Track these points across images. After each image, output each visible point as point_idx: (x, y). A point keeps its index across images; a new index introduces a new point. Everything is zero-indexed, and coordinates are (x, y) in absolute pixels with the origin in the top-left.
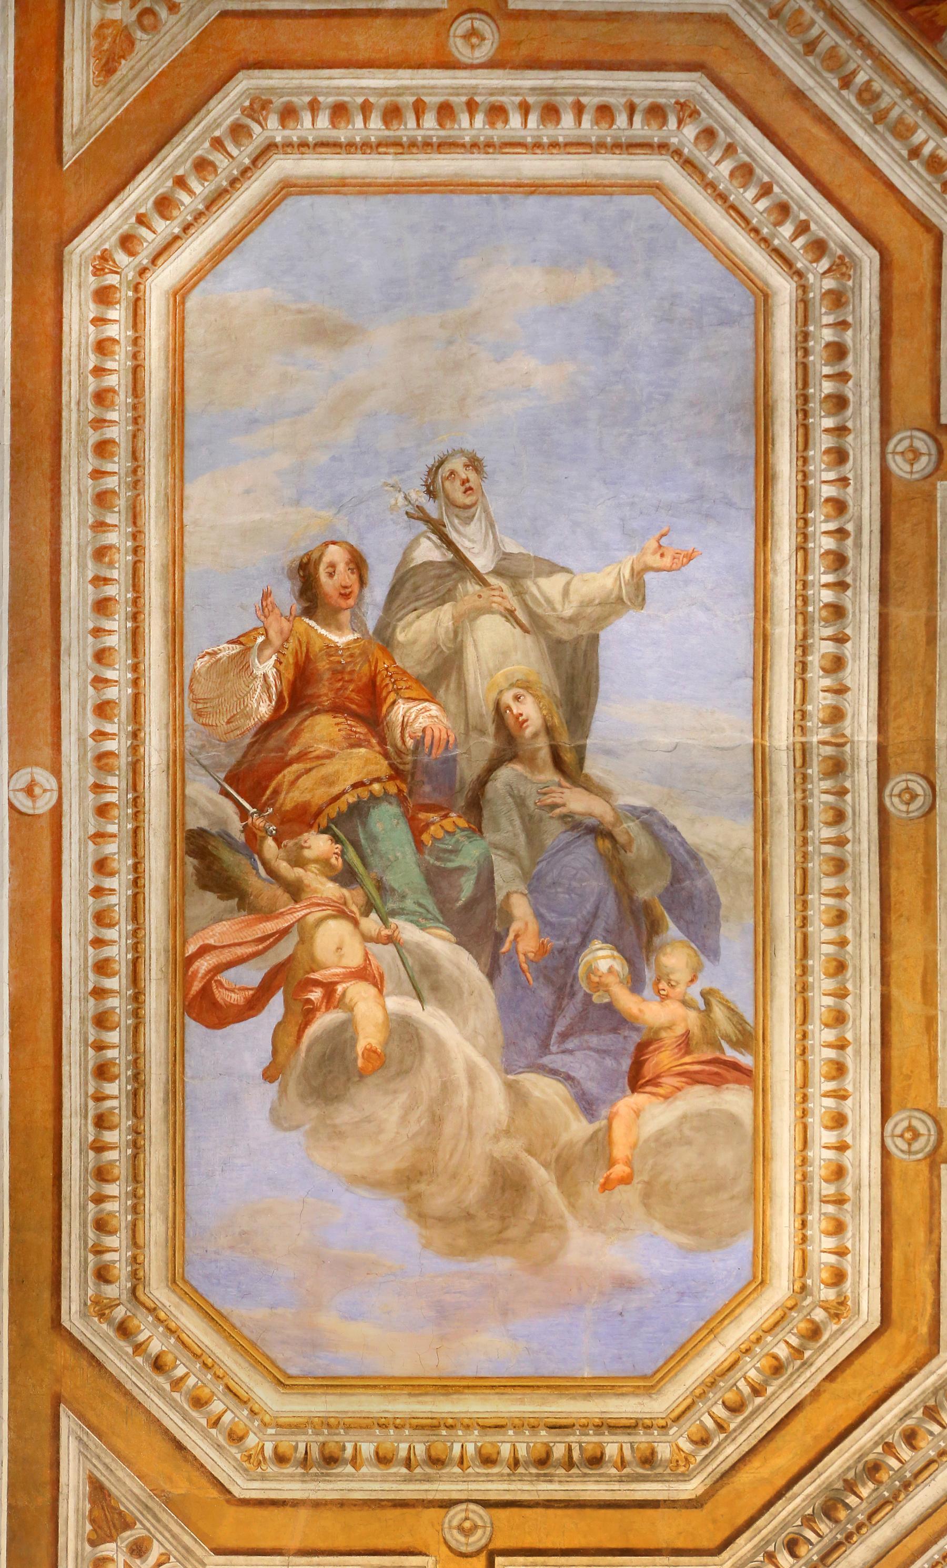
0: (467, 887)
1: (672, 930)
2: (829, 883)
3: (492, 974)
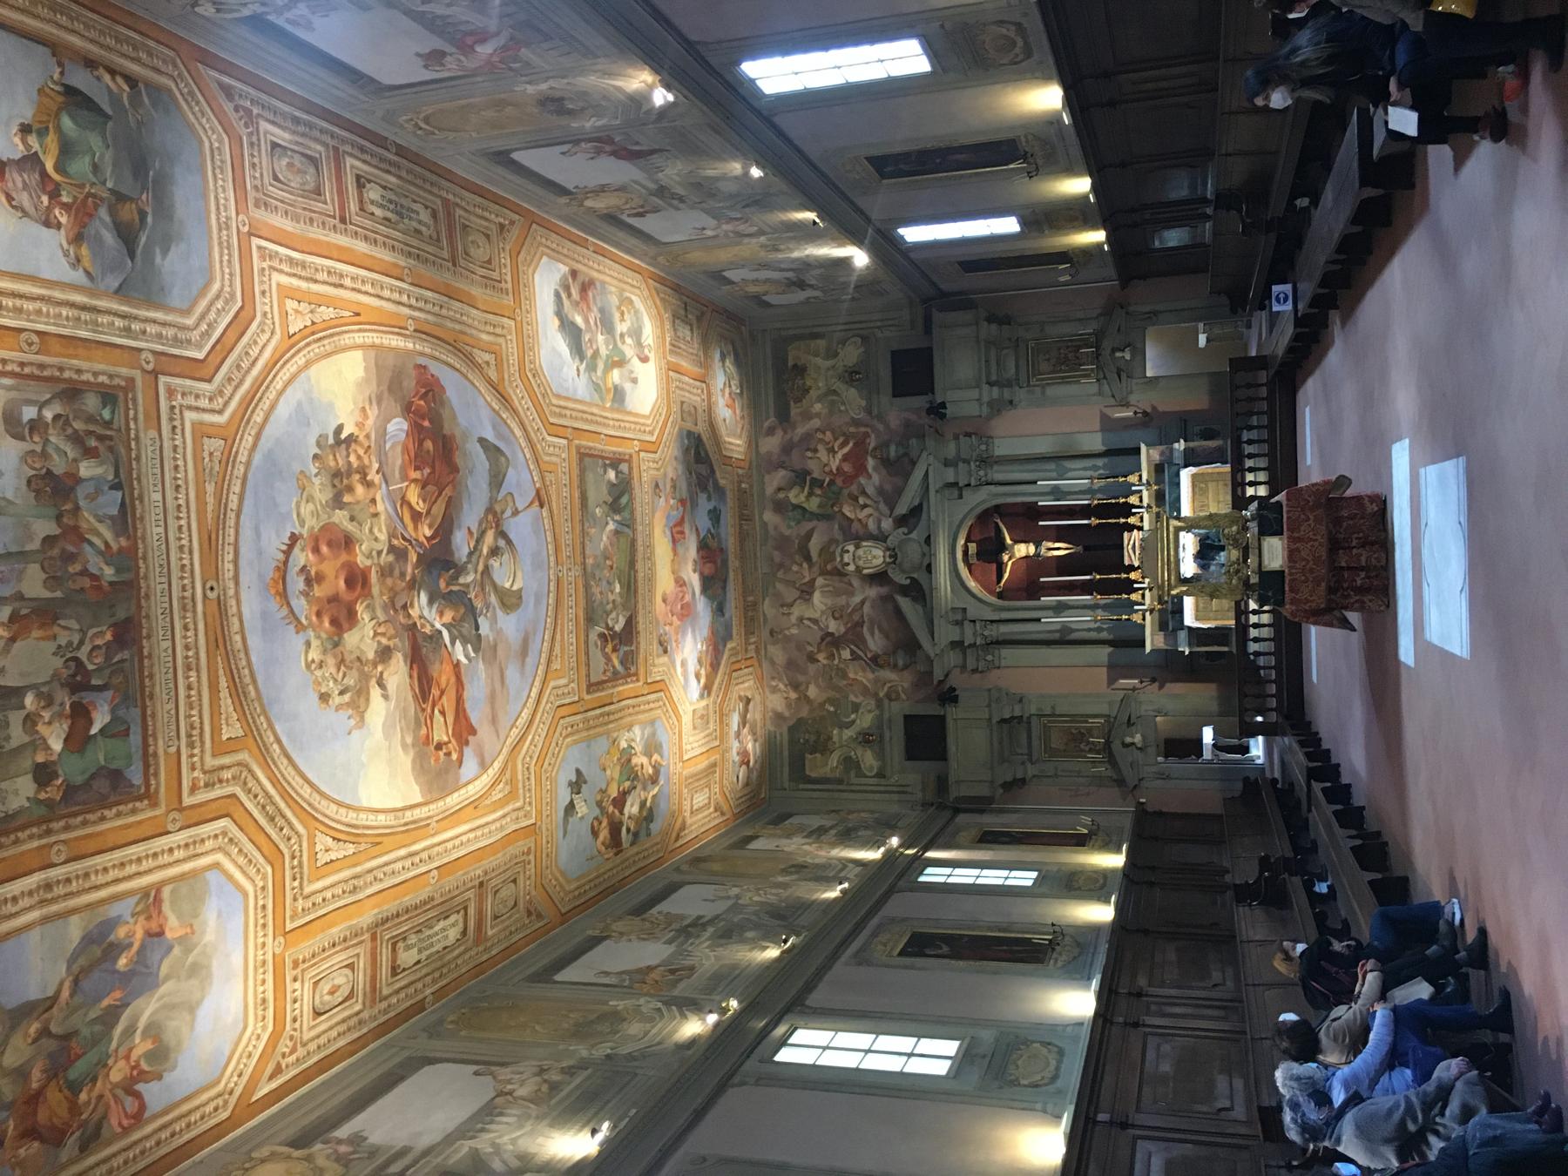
0: (97, 1028)
1: (112, 937)
2: (93, 877)
3: (128, 1005)
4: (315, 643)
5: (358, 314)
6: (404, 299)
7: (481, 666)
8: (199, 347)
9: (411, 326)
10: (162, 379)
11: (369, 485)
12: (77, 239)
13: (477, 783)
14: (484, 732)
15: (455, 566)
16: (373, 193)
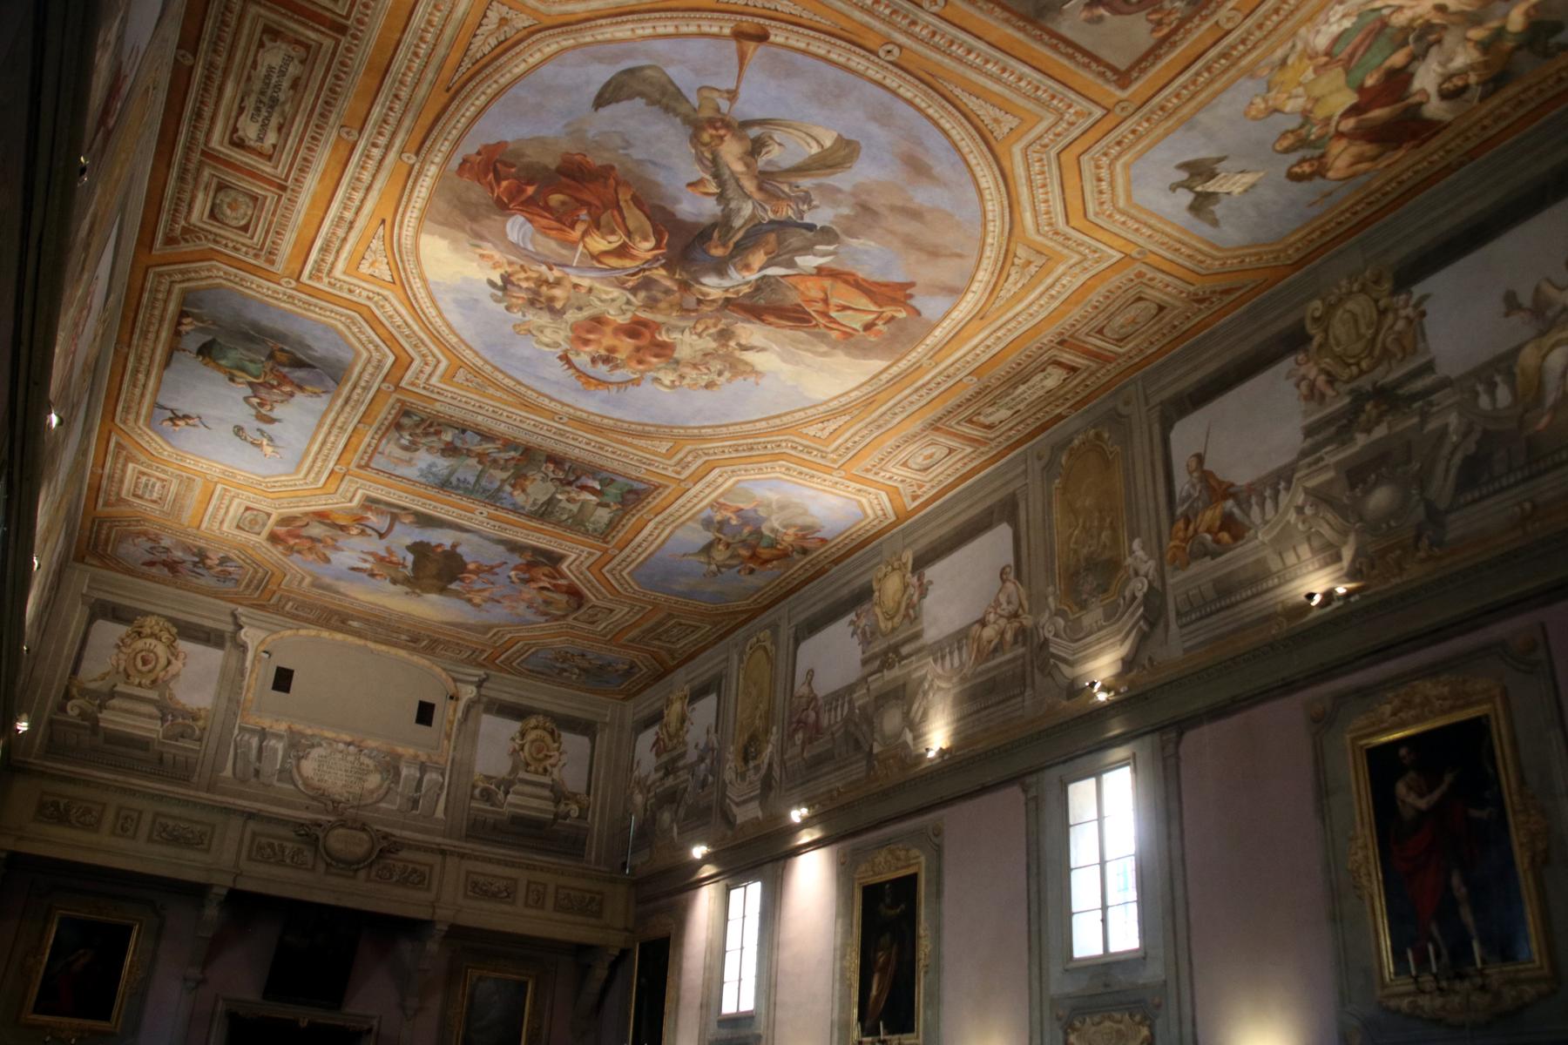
4: (661, 375)
5: (383, 221)
6: (376, 153)
7: (854, 242)
8: (385, 356)
9: (409, 158)
10: (403, 384)
11: (558, 283)
12: (301, 388)
13: (960, 308)
14: (925, 273)
15: (714, 226)
16: (250, 131)
